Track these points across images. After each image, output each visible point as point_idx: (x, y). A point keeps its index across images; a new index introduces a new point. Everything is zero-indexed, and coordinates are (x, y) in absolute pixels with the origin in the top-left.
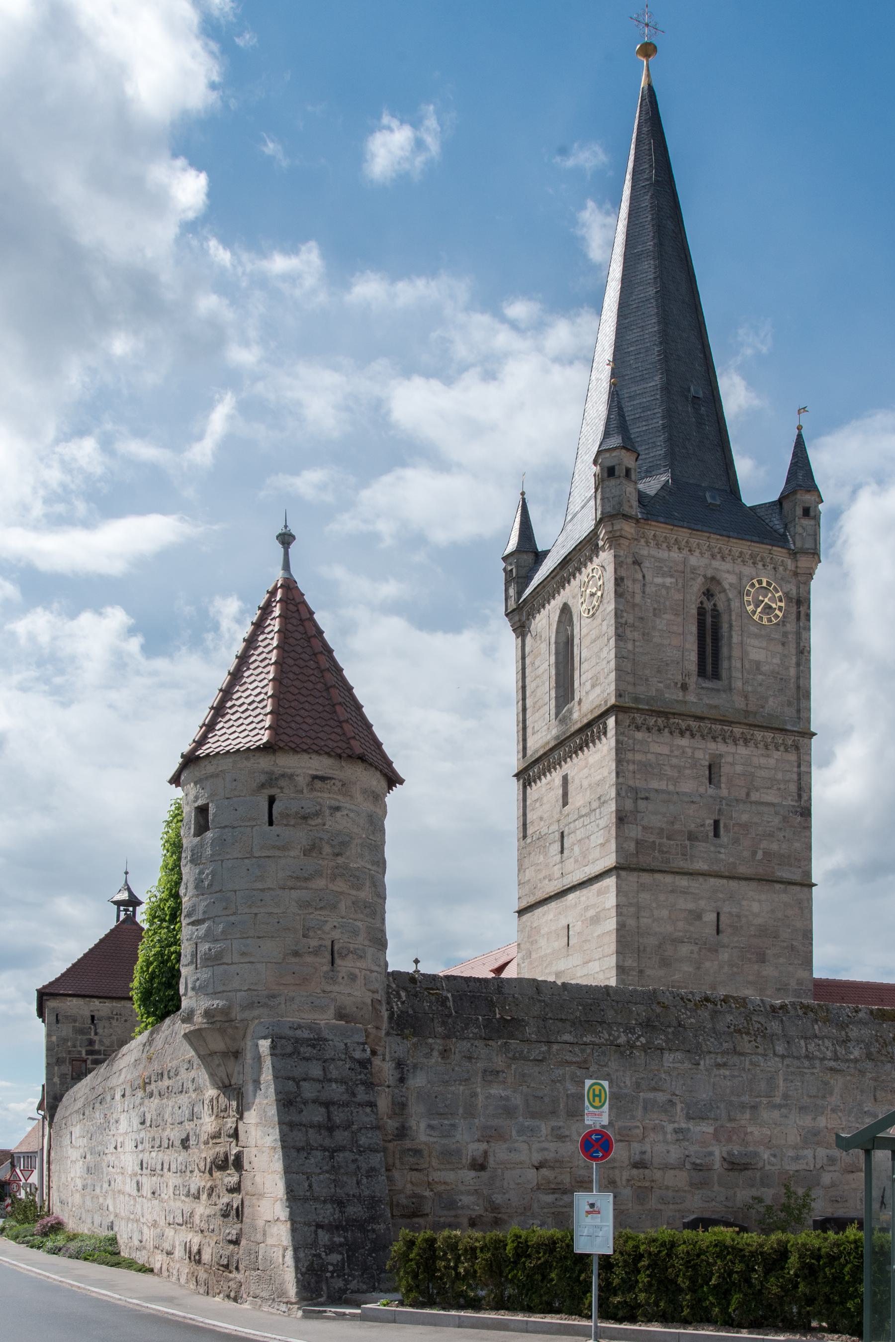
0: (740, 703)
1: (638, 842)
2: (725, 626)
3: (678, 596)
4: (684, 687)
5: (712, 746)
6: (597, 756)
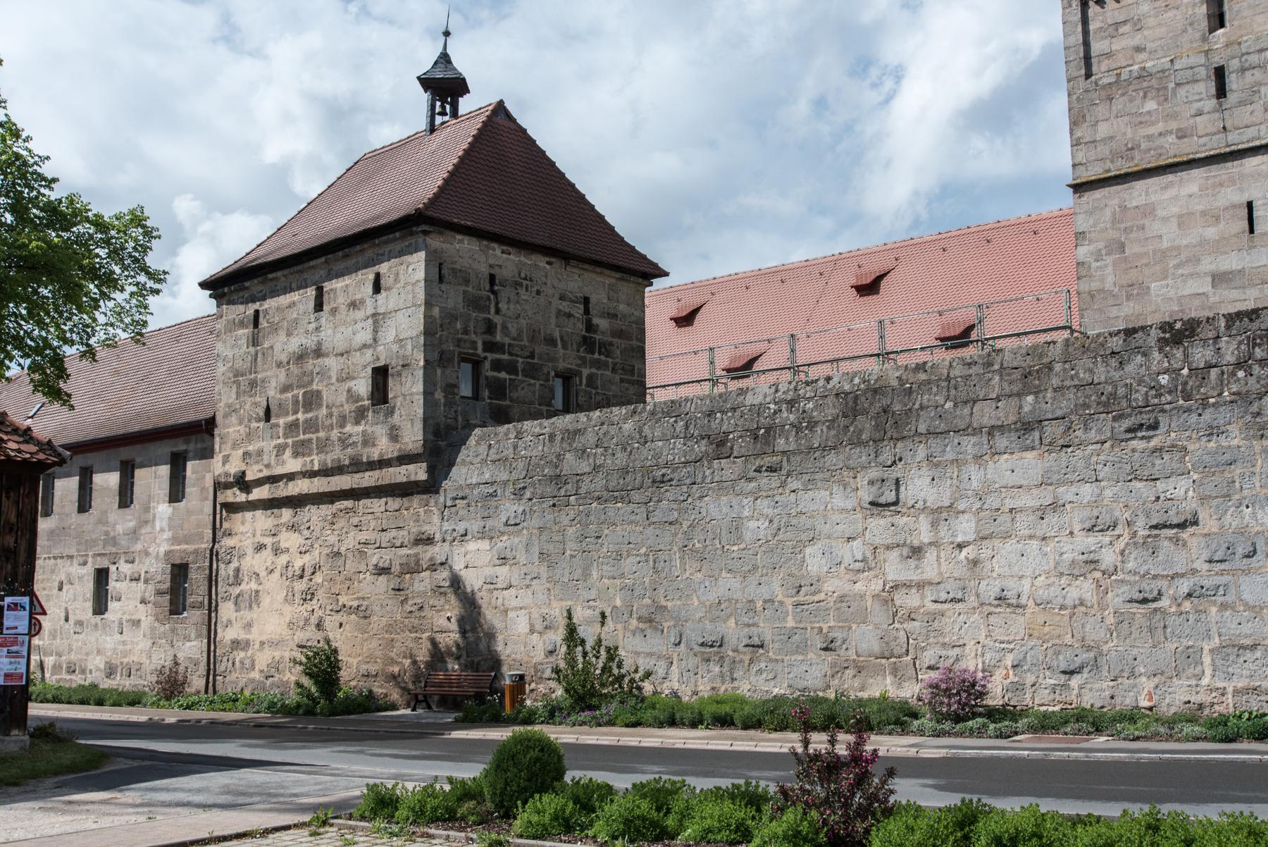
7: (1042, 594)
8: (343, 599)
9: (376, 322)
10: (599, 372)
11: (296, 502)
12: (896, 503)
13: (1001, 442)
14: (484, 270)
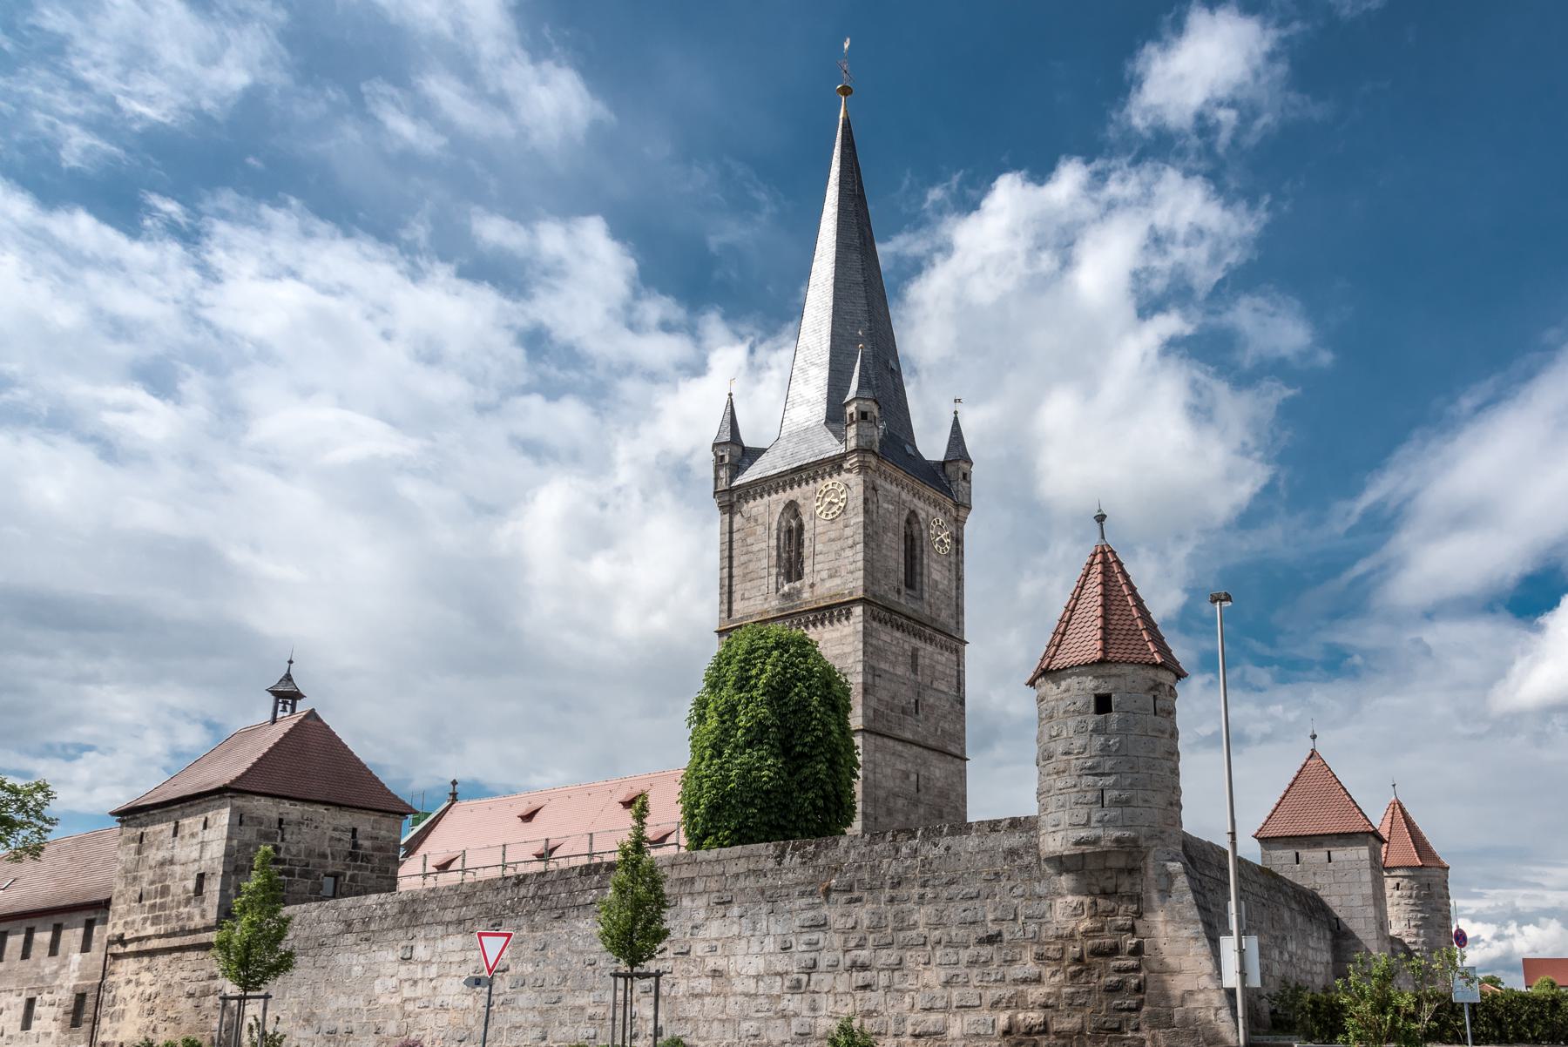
0: (927, 611)
1: (875, 711)
2: (918, 549)
3: (896, 521)
4: (899, 592)
5: (913, 640)
6: (836, 634)
7: (456, 1003)
8: (169, 1013)
9: (202, 847)
11: (152, 953)
12: (410, 958)
13: (451, 929)
14: (275, 815)
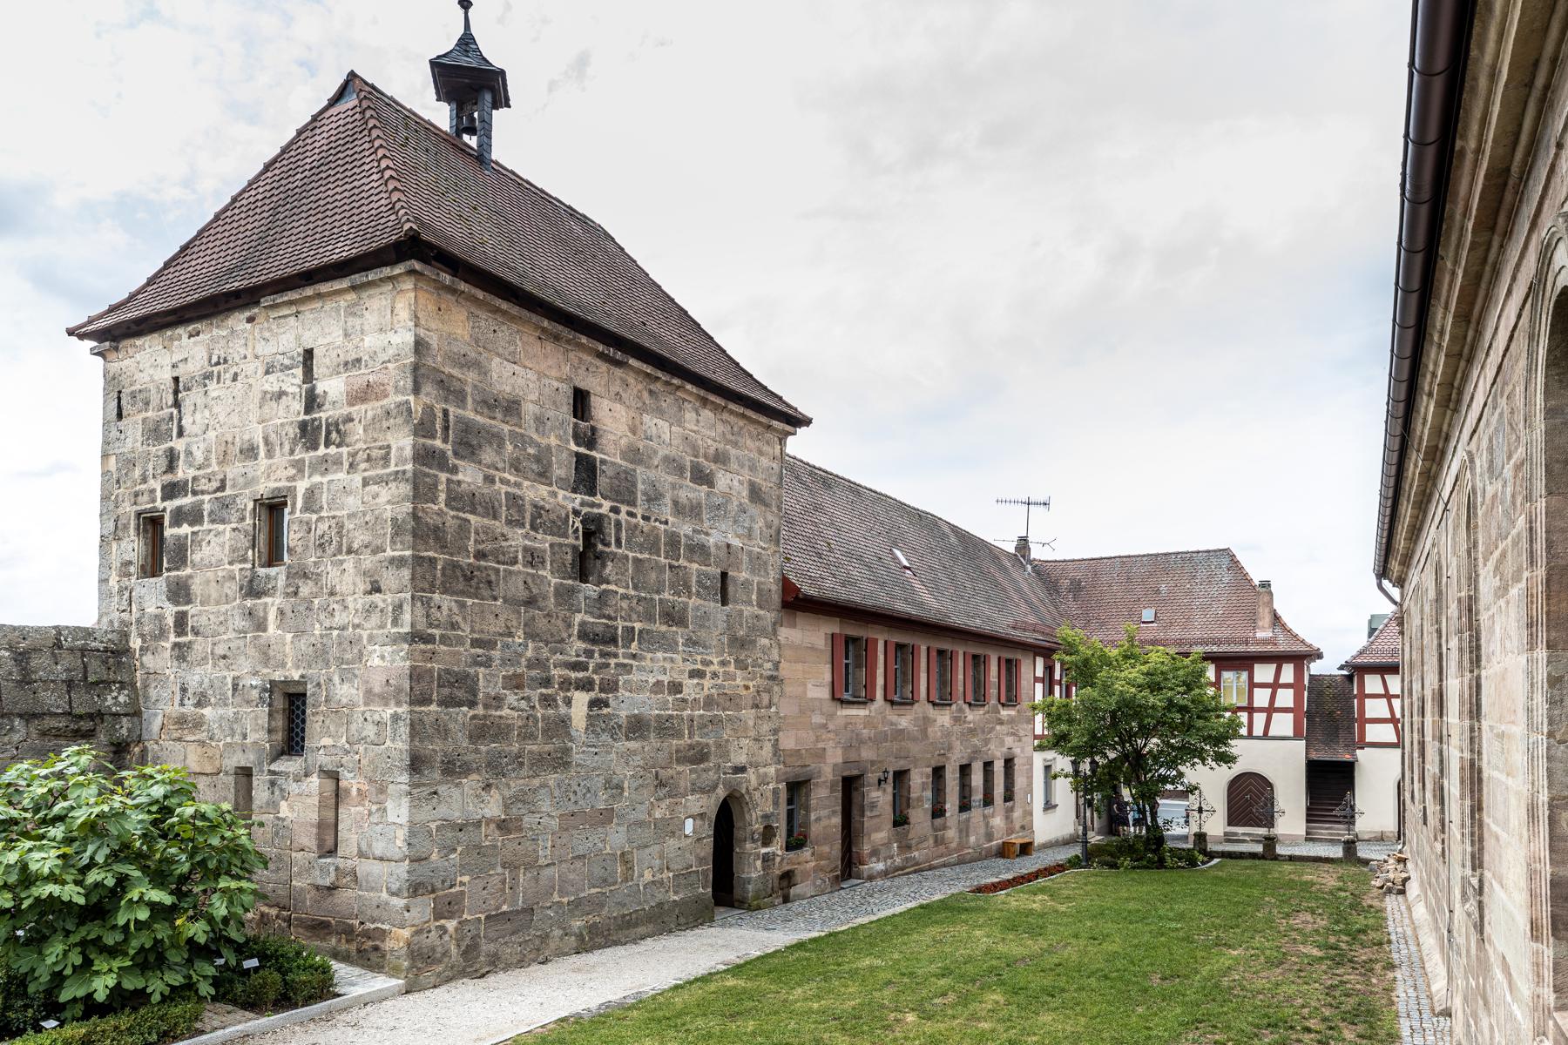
10: (325, 480)
